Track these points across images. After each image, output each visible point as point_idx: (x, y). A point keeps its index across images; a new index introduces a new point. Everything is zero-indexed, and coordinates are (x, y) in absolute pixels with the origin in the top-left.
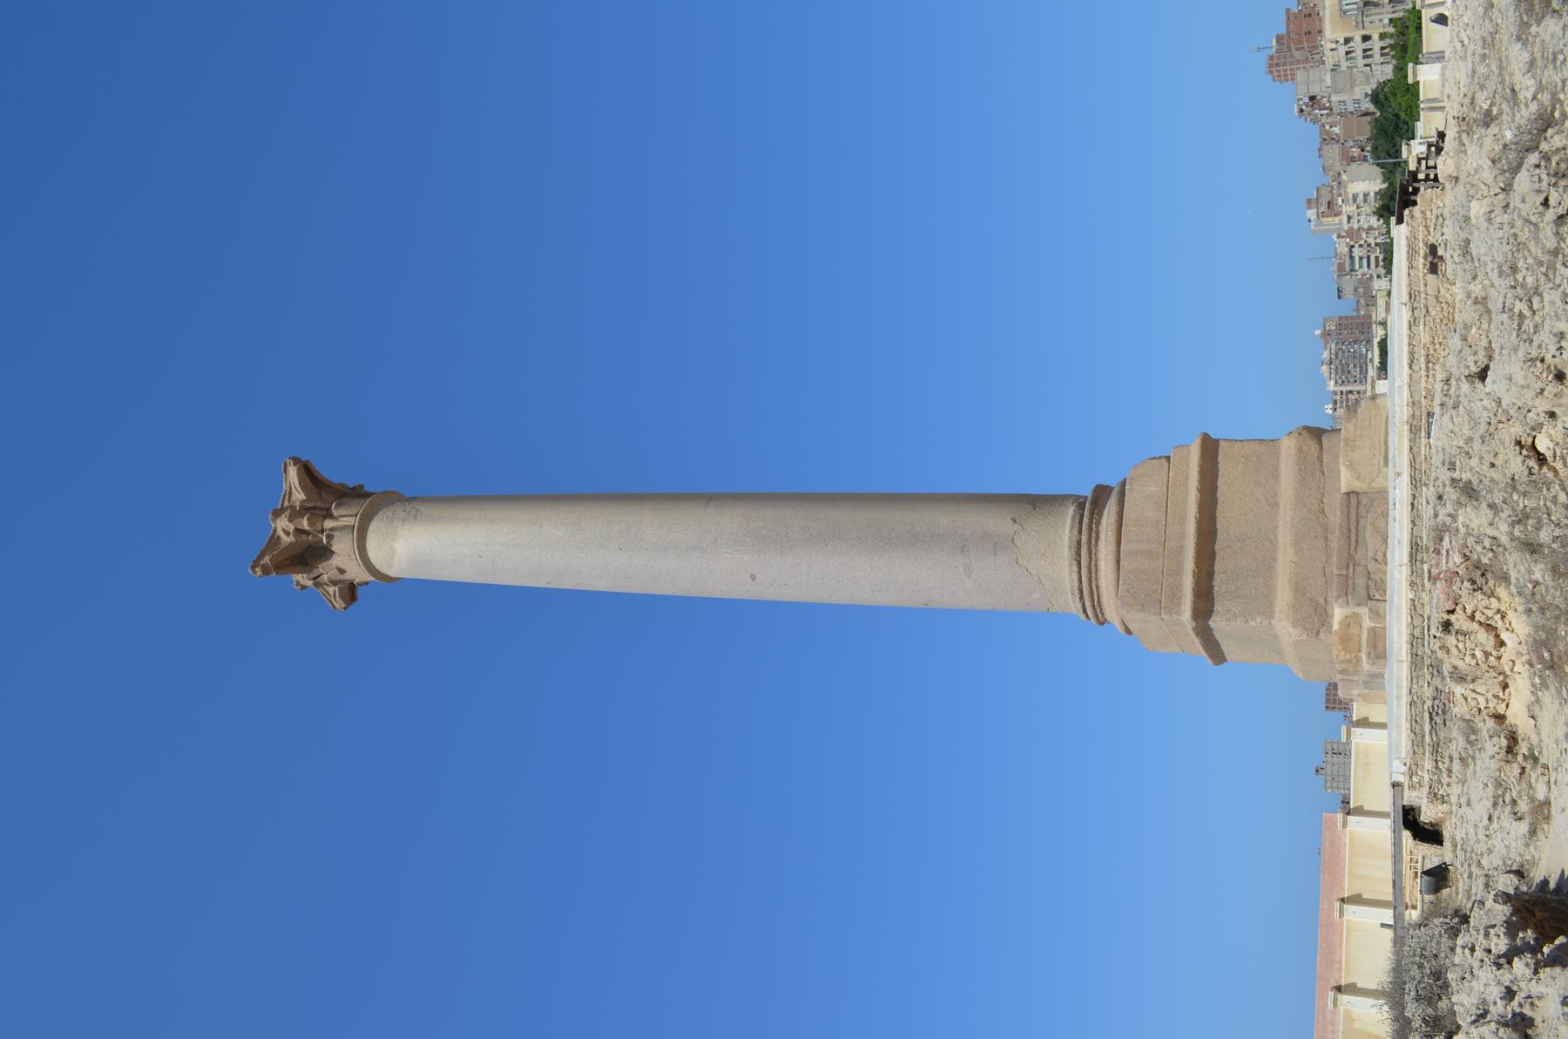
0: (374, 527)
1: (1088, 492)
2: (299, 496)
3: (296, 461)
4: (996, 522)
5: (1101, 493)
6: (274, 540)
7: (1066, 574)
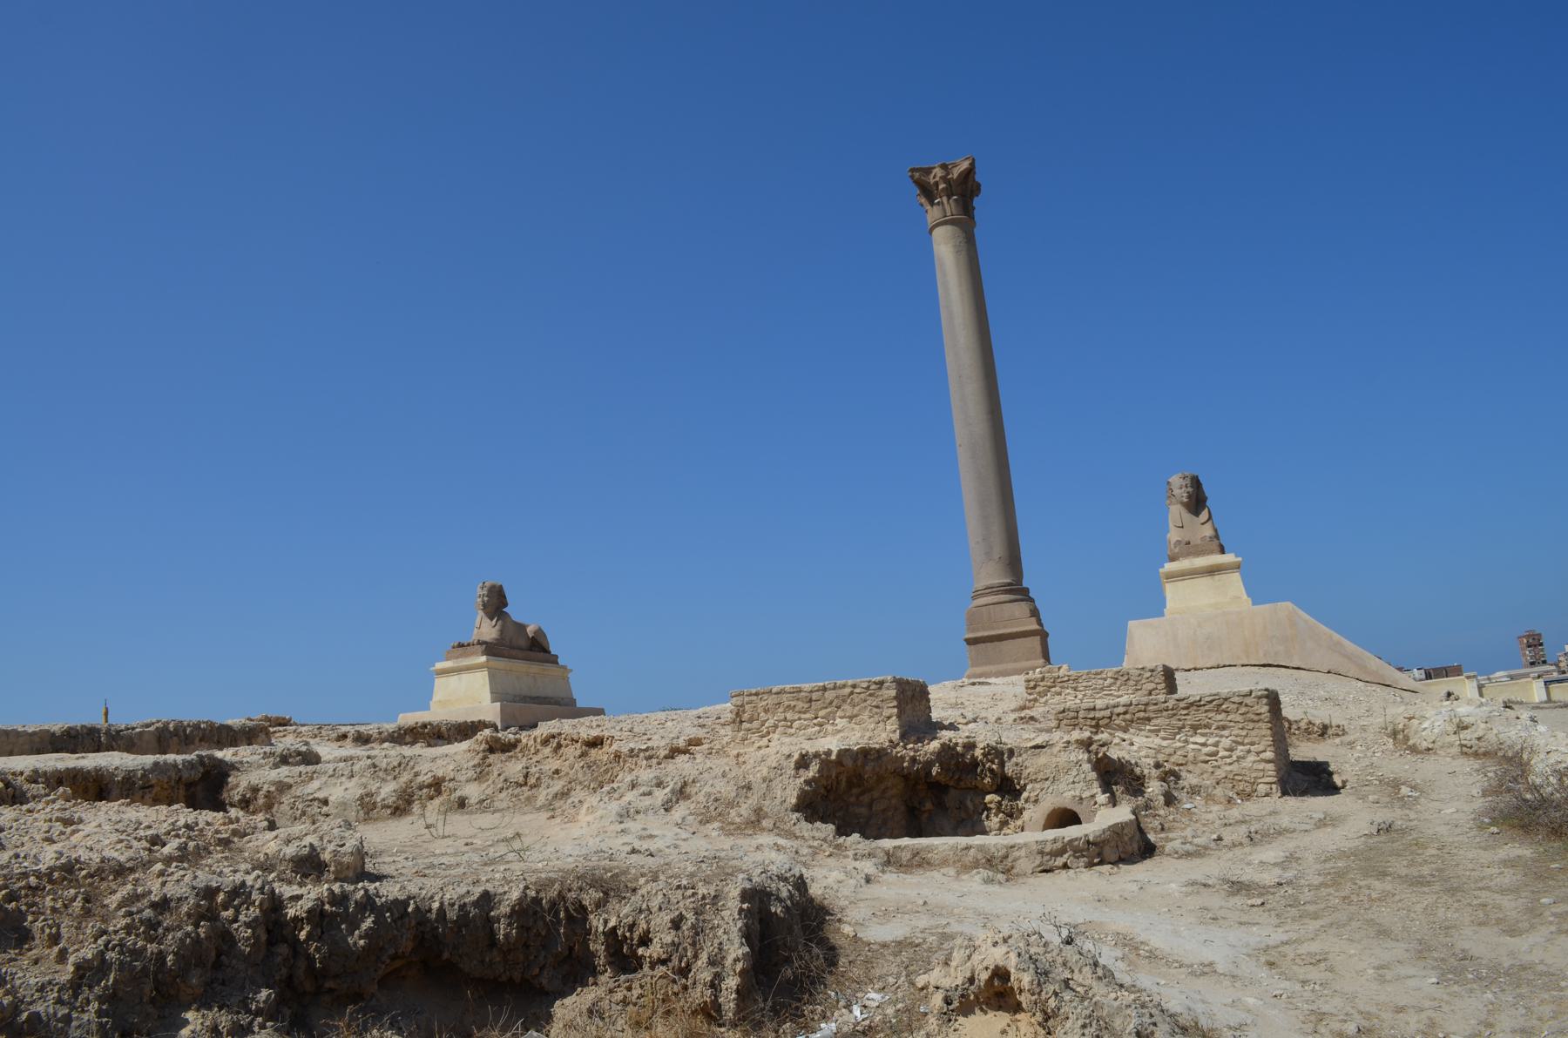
0: (949, 228)
1: (1025, 584)
2: (955, 173)
3: (972, 164)
4: (999, 550)
5: (1025, 592)
6: (928, 171)
7: (981, 584)
